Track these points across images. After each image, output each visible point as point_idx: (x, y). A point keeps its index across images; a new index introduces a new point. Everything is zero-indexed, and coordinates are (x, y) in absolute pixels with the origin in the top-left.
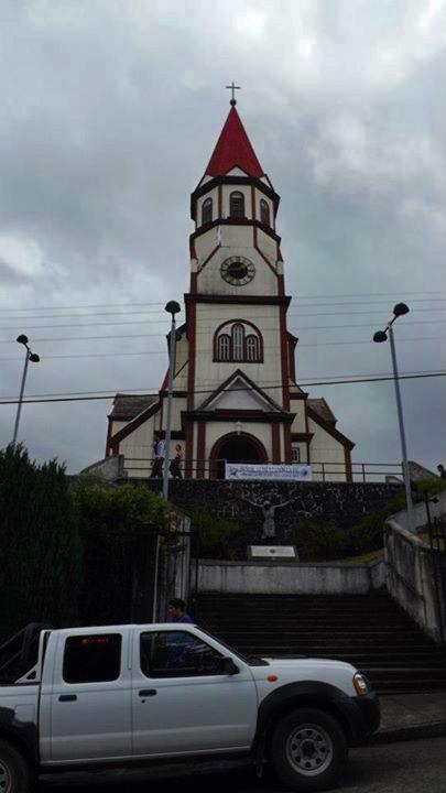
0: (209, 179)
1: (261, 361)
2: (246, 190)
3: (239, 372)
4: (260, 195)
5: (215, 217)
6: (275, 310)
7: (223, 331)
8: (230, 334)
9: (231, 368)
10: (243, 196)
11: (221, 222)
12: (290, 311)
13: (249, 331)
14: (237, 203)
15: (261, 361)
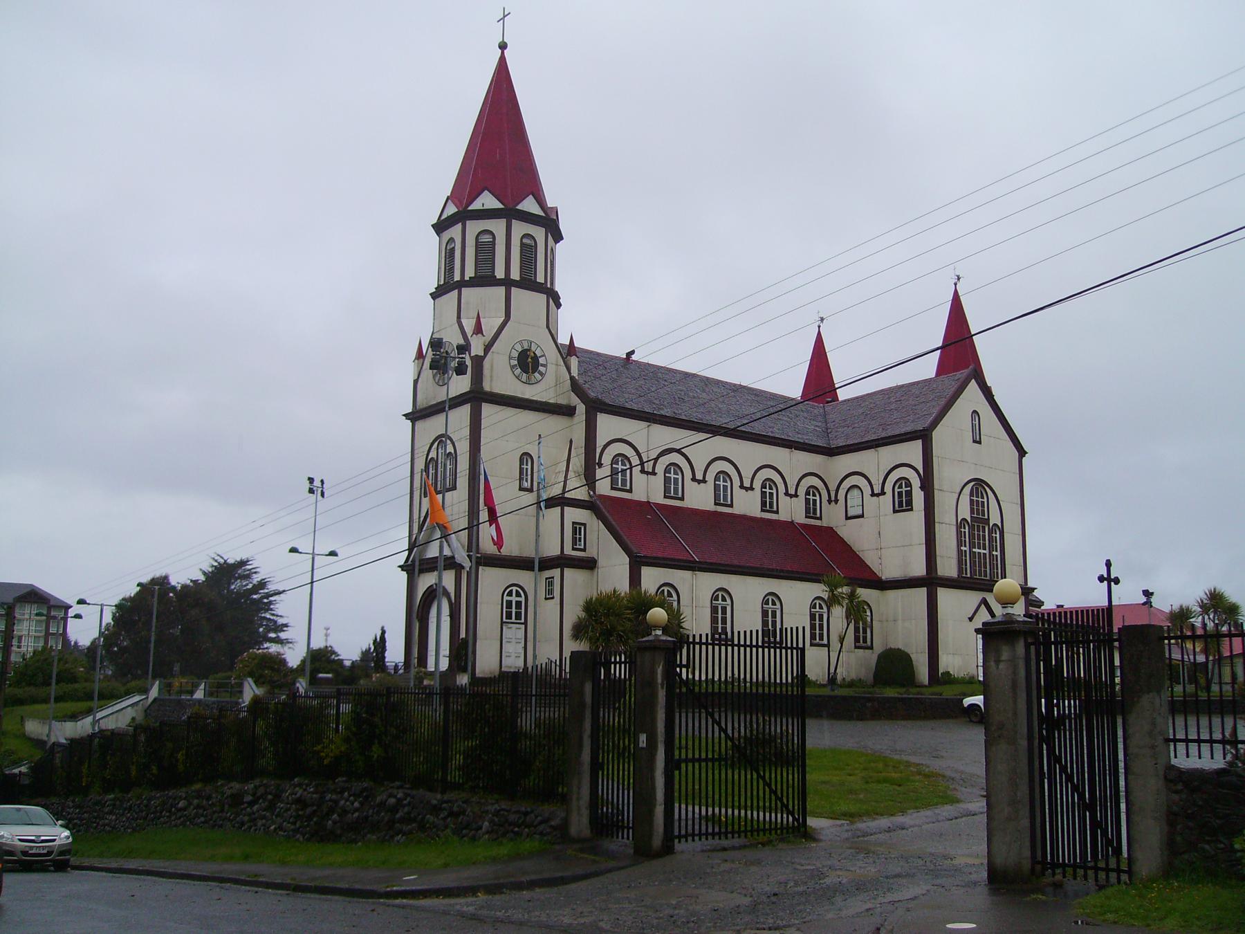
0: (452, 209)
2: (498, 227)
5: (457, 277)
10: (494, 237)
11: (462, 284)
14: (485, 251)
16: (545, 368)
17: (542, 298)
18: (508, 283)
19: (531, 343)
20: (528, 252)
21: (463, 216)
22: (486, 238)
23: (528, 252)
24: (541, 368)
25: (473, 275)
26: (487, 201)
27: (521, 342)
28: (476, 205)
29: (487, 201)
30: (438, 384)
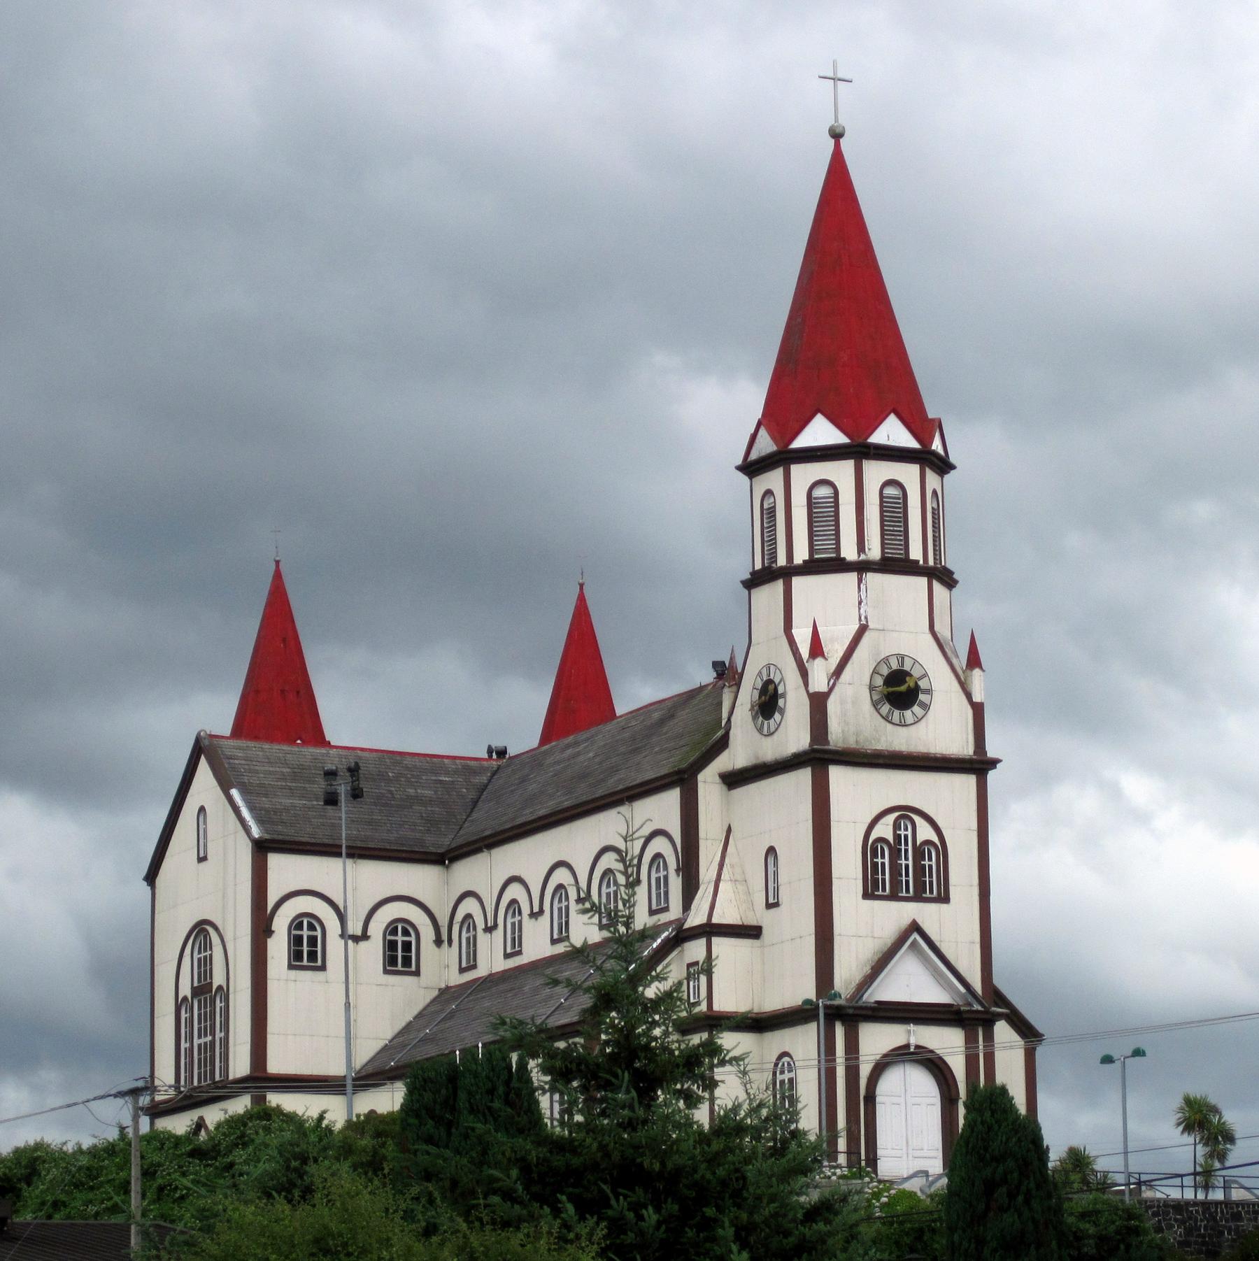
1: (944, 898)
2: (841, 472)
3: (915, 927)
4: (877, 472)
5: (782, 561)
6: (970, 781)
7: (879, 832)
8: (890, 838)
9: (906, 912)
11: (789, 572)
12: (992, 776)
13: (925, 833)
15: (944, 898)
16: (929, 696)
17: (923, 581)
18: (862, 568)
19: (903, 658)
20: (894, 513)
21: (785, 458)
22: (822, 492)
23: (894, 513)
24: (922, 697)
25: (807, 558)
26: (820, 432)
27: (886, 660)
28: (802, 442)
29: (820, 432)
30: (760, 730)
